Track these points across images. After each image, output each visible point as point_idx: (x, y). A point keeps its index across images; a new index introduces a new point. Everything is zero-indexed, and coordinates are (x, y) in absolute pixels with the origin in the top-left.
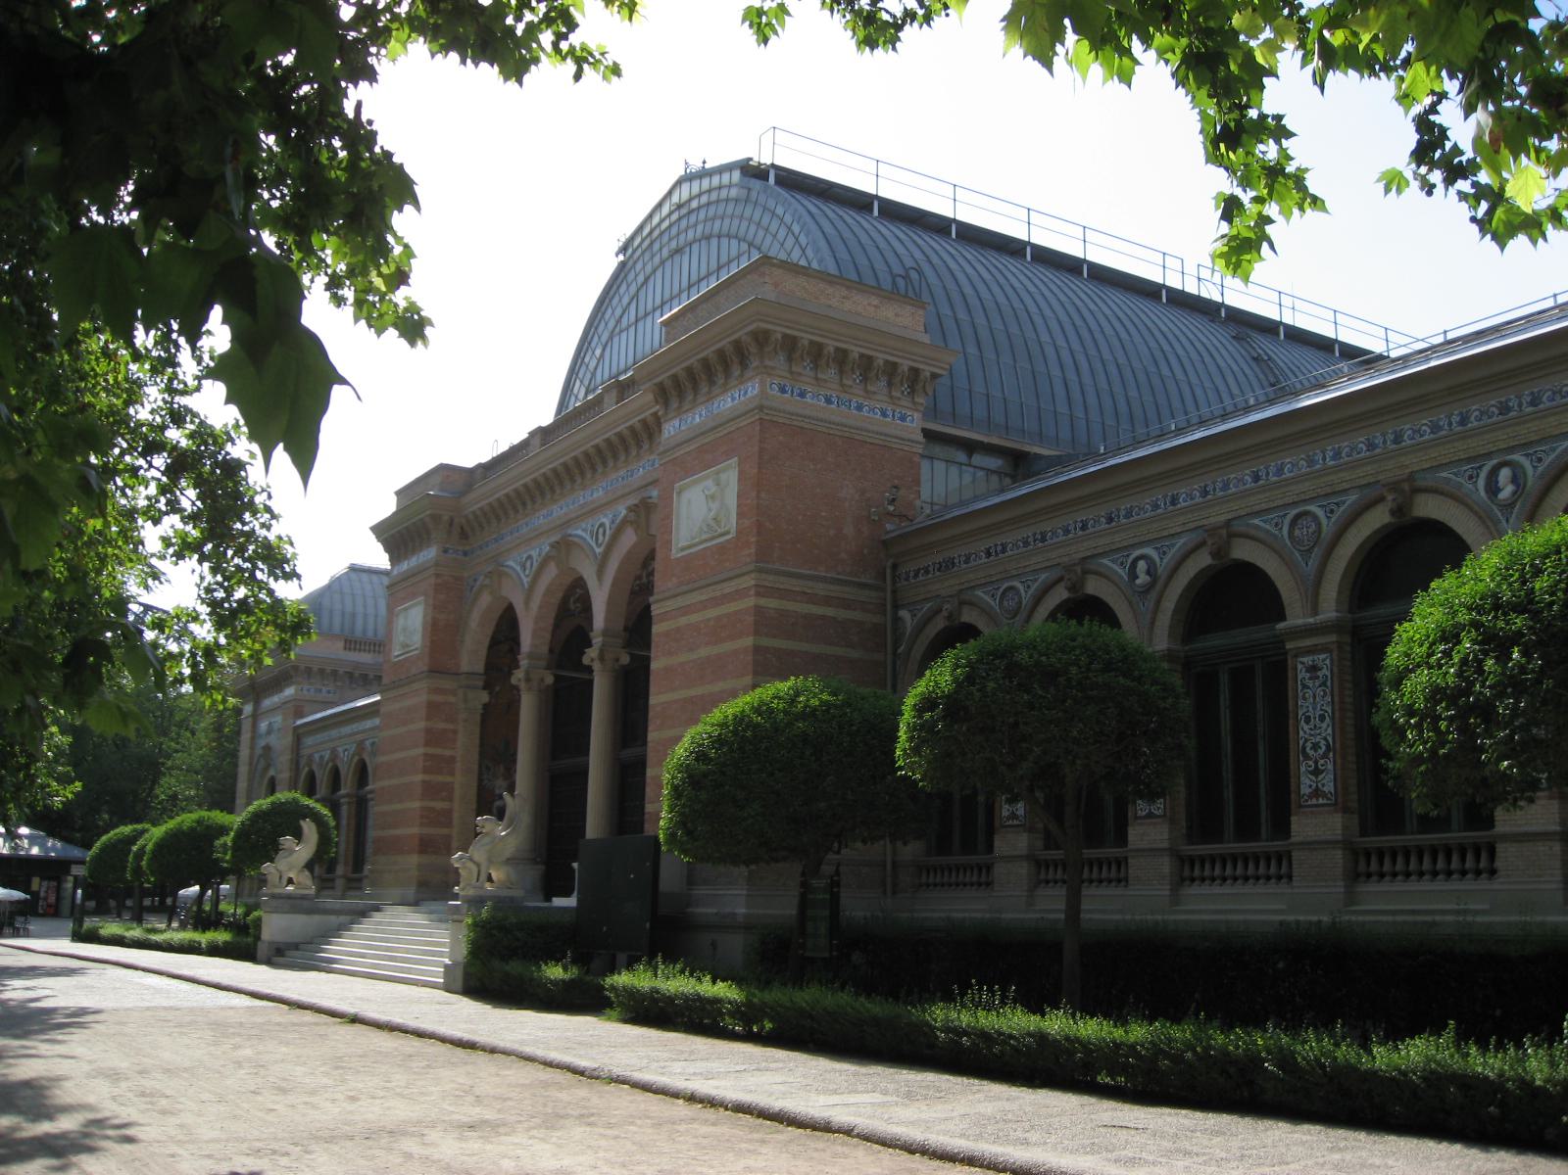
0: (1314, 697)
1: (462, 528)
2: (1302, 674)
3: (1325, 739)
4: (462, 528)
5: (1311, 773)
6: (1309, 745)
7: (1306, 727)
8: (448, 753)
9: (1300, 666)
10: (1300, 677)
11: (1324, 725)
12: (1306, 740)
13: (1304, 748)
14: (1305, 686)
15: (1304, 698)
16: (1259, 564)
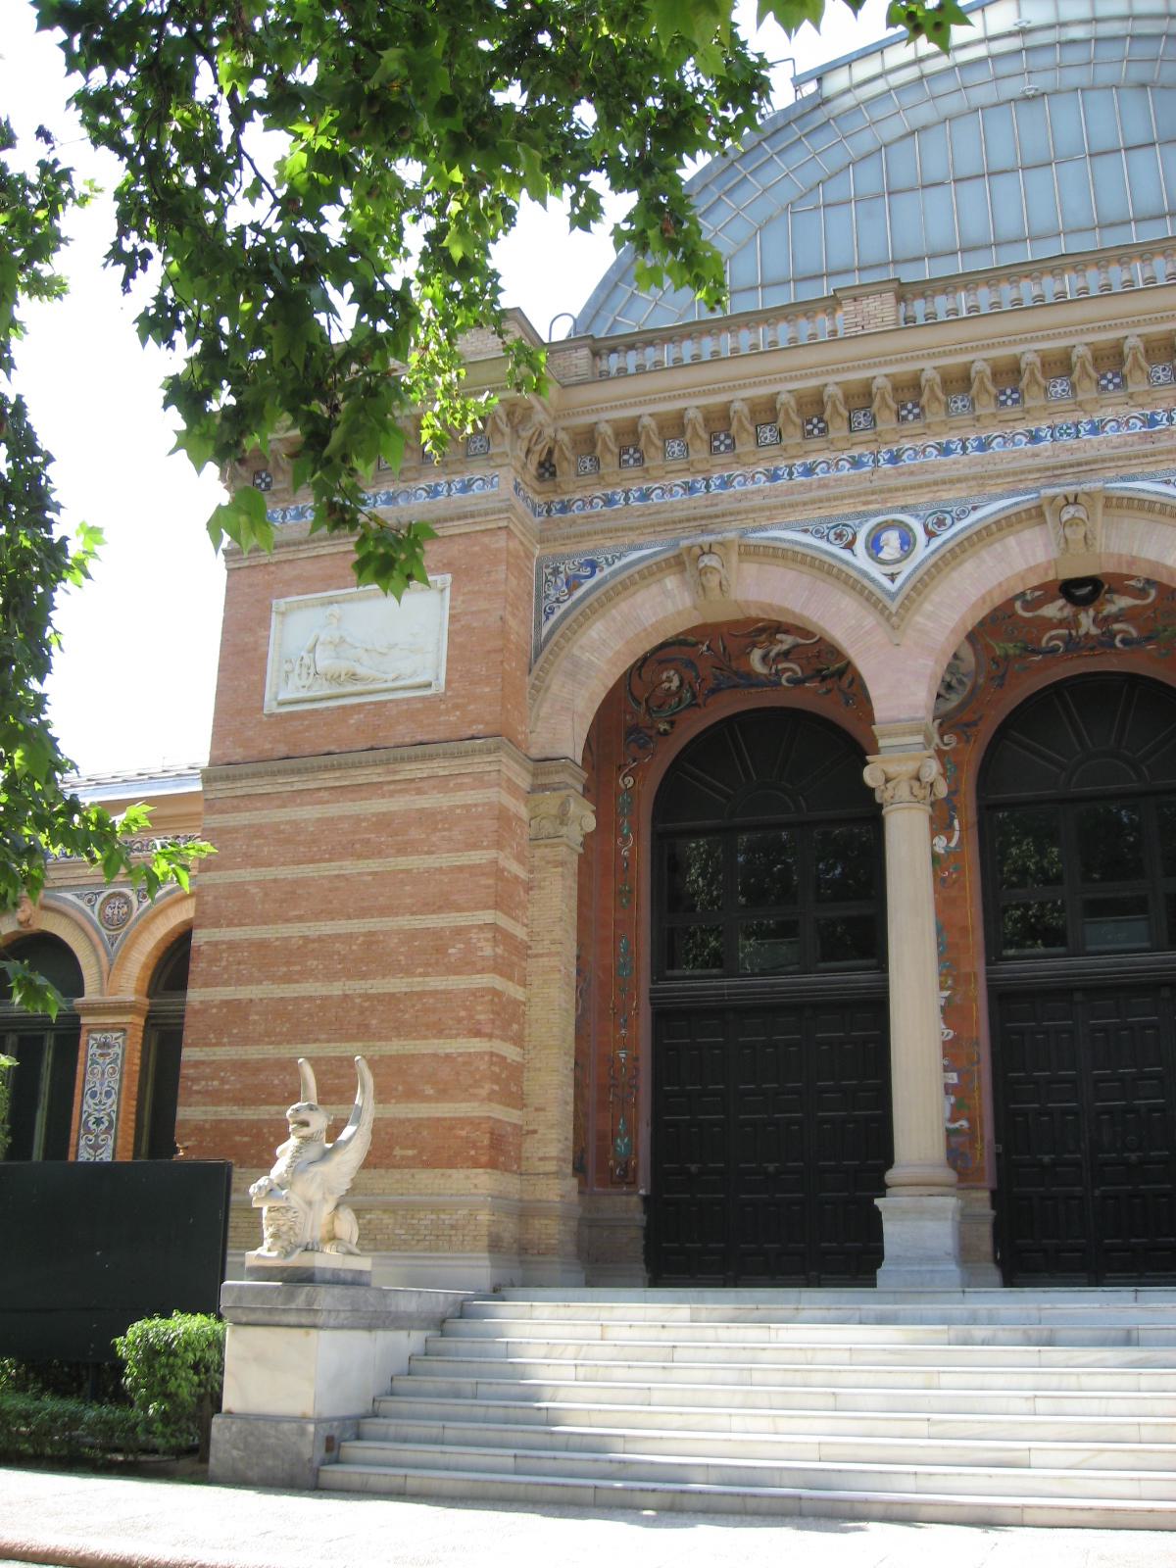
0: (103, 1074)
1: (550, 452)
2: (93, 1050)
3: (109, 1115)
4: (550, 452)
5: (91, 1147)
6: (92, 1119)
7: (91, 1102)
8: (521, 933)
9: (92, 1042)
10: (91, 1052)
11: (110, 1101)
12: (90, 1115)
13: (86, 1122)
14: (95, 1062)
15: (92, 1073)
16: (54, 931)
